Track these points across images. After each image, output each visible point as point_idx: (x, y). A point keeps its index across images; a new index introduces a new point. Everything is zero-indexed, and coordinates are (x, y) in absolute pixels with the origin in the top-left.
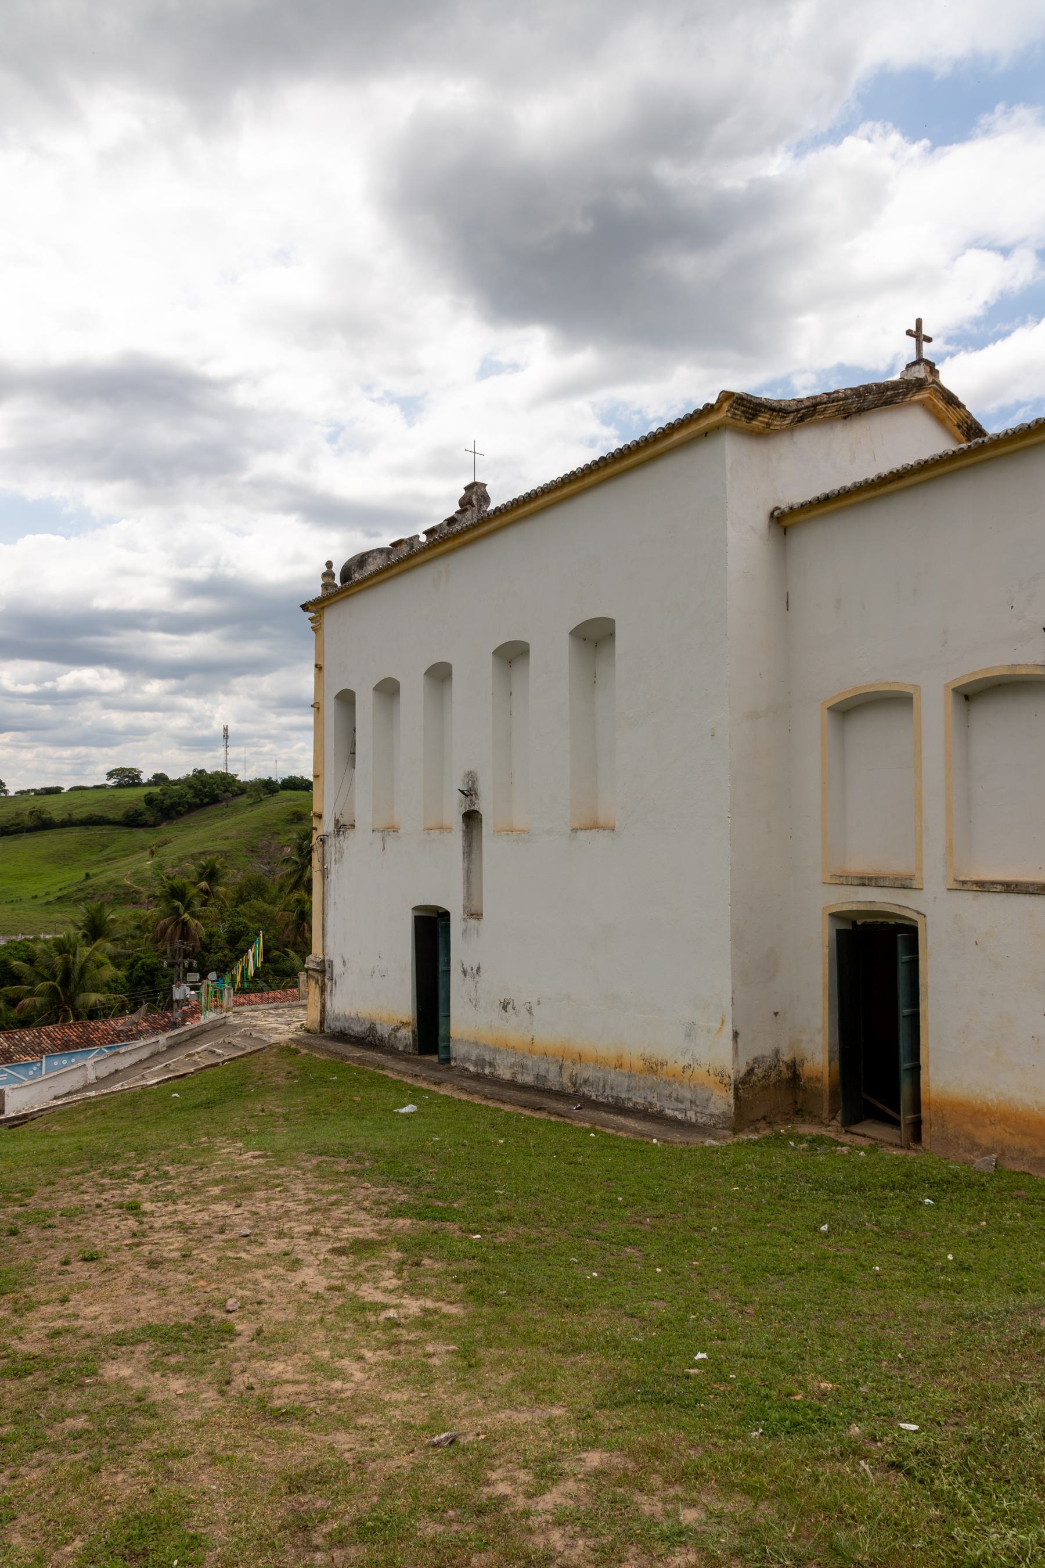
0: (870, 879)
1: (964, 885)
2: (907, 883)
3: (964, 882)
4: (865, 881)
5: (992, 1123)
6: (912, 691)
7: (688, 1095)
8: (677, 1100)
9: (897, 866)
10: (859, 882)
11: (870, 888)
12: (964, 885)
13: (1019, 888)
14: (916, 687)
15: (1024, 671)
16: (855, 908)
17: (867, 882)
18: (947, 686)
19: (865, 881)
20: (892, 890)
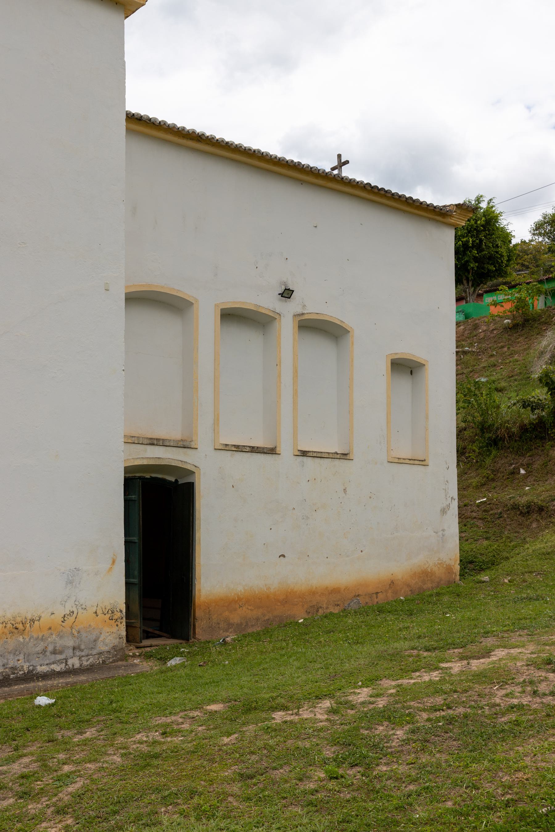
0: (158, 440)
1: (226, 448)
2: (186, 444)
3: (226, 445)
4: (154, 442)
5: (240, 607)
6: (193, 302)
7: (70, 643)
8: (54, 652)
9: (171, 431)
10: (148, 442)
11: (157, 447)
12: (226, 448)
13: (259, 449)
14: (197, 300)
15: (263, 311)
16: (145, 462)
17: (155, 442)
18: (216, 306)
19: (154, 442)
20: (174, 449)
